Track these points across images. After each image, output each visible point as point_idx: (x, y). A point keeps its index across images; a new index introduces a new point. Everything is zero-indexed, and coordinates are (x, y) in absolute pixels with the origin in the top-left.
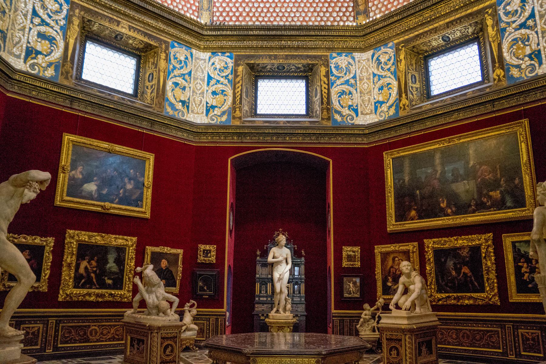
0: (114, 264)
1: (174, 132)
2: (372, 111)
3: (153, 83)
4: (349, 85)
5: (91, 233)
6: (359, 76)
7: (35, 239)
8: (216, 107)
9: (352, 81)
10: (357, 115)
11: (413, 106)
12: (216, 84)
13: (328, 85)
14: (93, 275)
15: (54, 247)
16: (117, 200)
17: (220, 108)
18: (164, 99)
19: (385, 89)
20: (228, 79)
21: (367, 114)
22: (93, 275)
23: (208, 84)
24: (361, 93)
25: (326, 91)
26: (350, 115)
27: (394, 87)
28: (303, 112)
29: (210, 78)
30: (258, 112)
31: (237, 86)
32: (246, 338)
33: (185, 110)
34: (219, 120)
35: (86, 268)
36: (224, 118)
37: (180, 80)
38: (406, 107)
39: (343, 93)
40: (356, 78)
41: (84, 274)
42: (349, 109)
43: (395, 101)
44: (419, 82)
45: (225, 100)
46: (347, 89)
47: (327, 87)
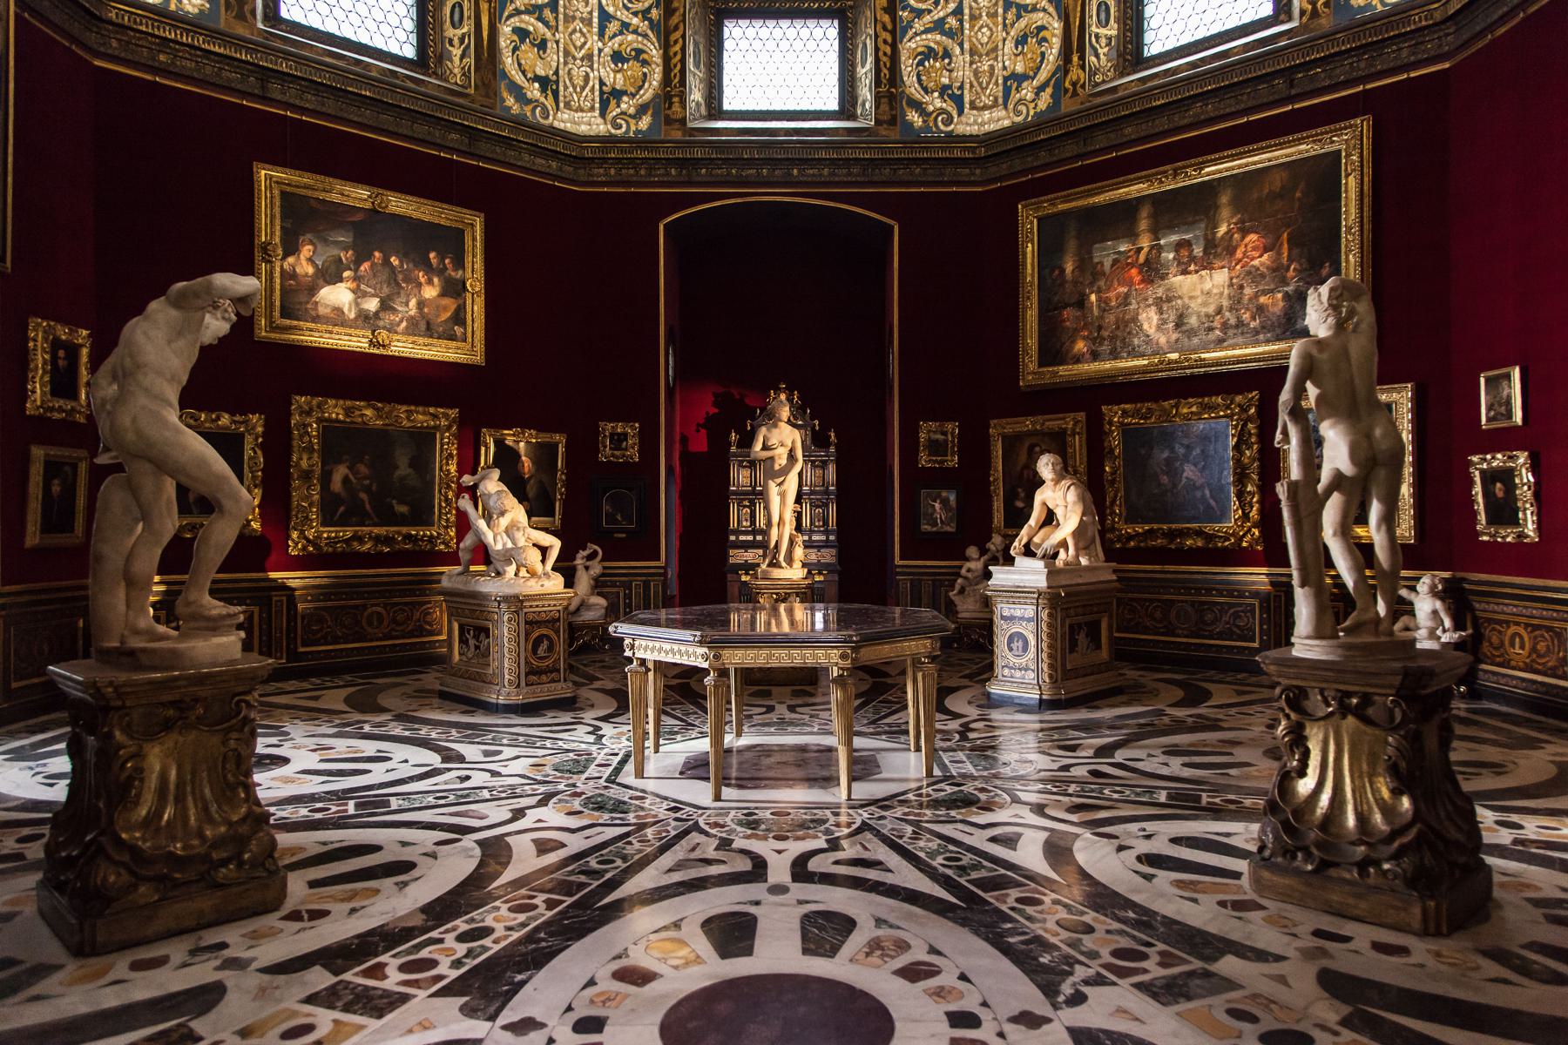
0: (409, 471)
1: (526, 157)
2: (996, 99)
3: (465, 30)
4: (943, 33)
5: (349, 403)
6: (971, 8)
7: (218, 418)
8: (624, 93)
9: (952, 21)
10: (961, 112)
11: (1097, 84)
12: (621, 33)
13: (893, 32)
14: (363, 496)
15: (264, 435)
16: (404, 324)
17: (633, 95)
18: (494, 74)
19: (1032, 41)
20: (650, 20)
21: (985, 108)
22: (363, 496)
23: (601, 34)
24: (973, 52)
25: (888, 50)
26: (942, 111)
27: (1054, 35)
28: (833, 105)
29: (605, 17)
30: (726, 107)
31: (673, 38)
33: (550, 103)
34: (633, 128)
35: (346, 480)
36: (645, 123)
37: (530, 22)
38: (1080, 90)
39: (929, 53)
40: (962, 14)
41: (343, 494)
42: (941, 96)
43: (1054, 74)
44: (1117, 21)
45: (645, 75)
46: (937, 43)
47: (889, 39)
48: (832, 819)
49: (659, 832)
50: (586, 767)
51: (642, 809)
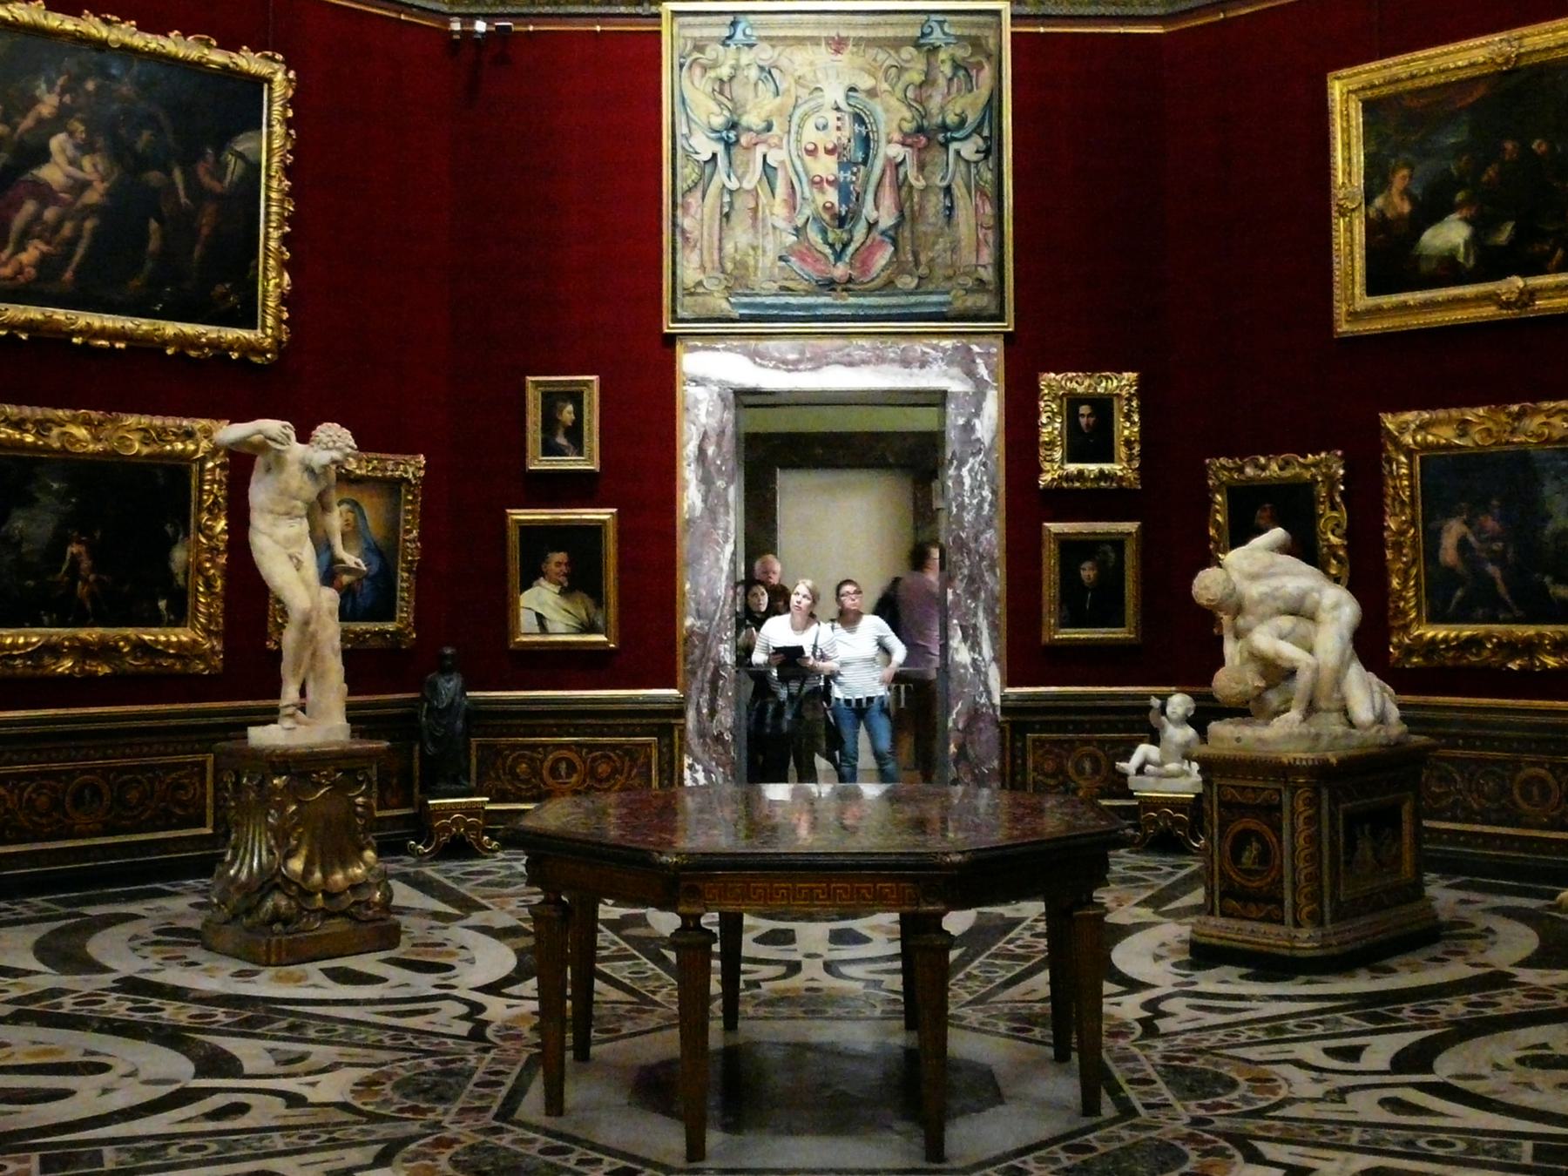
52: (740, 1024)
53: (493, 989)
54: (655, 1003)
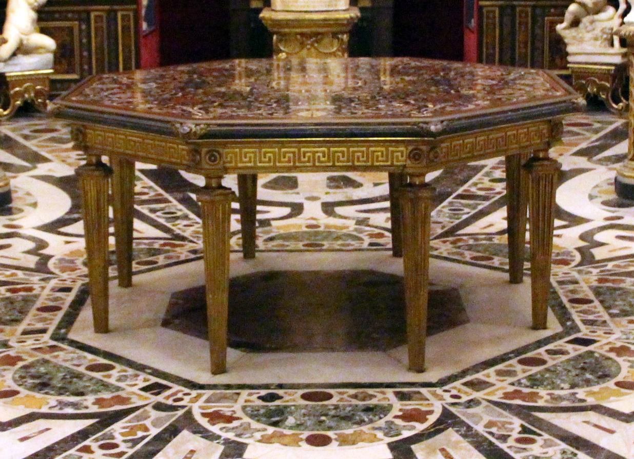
32: (191, 81)
48: (398, 406)
49: (133, 430)
50: (23, 312)
51: (106, 386)
52: (257, 254)
53: (54, 227)
54: (183, 239)
